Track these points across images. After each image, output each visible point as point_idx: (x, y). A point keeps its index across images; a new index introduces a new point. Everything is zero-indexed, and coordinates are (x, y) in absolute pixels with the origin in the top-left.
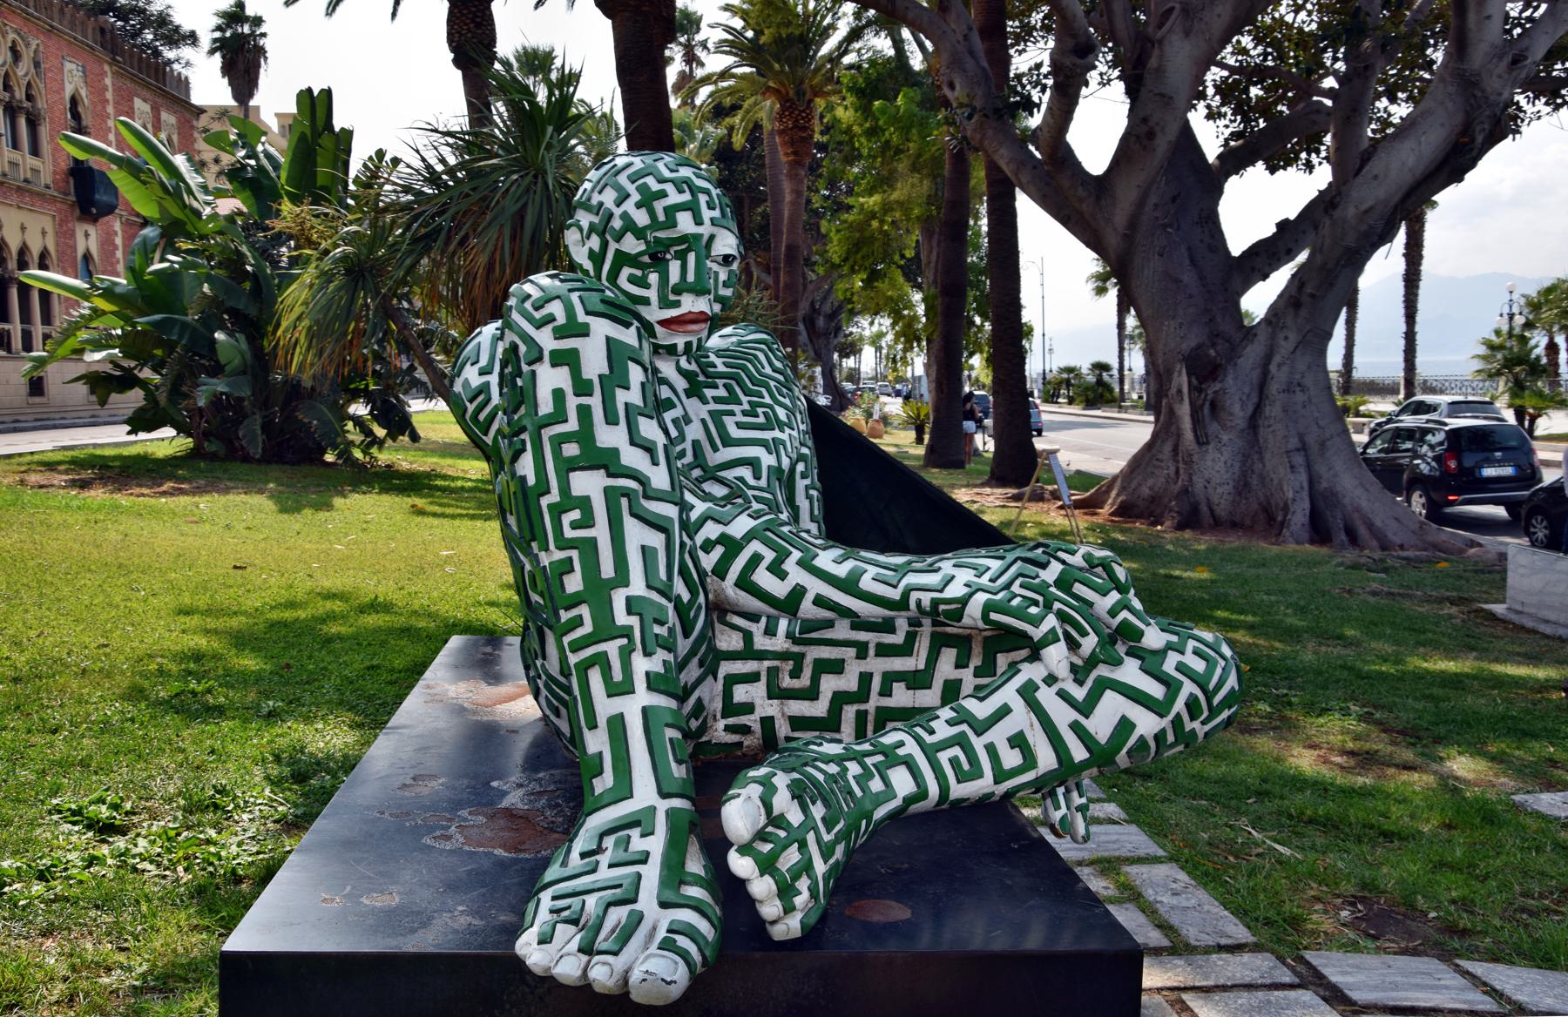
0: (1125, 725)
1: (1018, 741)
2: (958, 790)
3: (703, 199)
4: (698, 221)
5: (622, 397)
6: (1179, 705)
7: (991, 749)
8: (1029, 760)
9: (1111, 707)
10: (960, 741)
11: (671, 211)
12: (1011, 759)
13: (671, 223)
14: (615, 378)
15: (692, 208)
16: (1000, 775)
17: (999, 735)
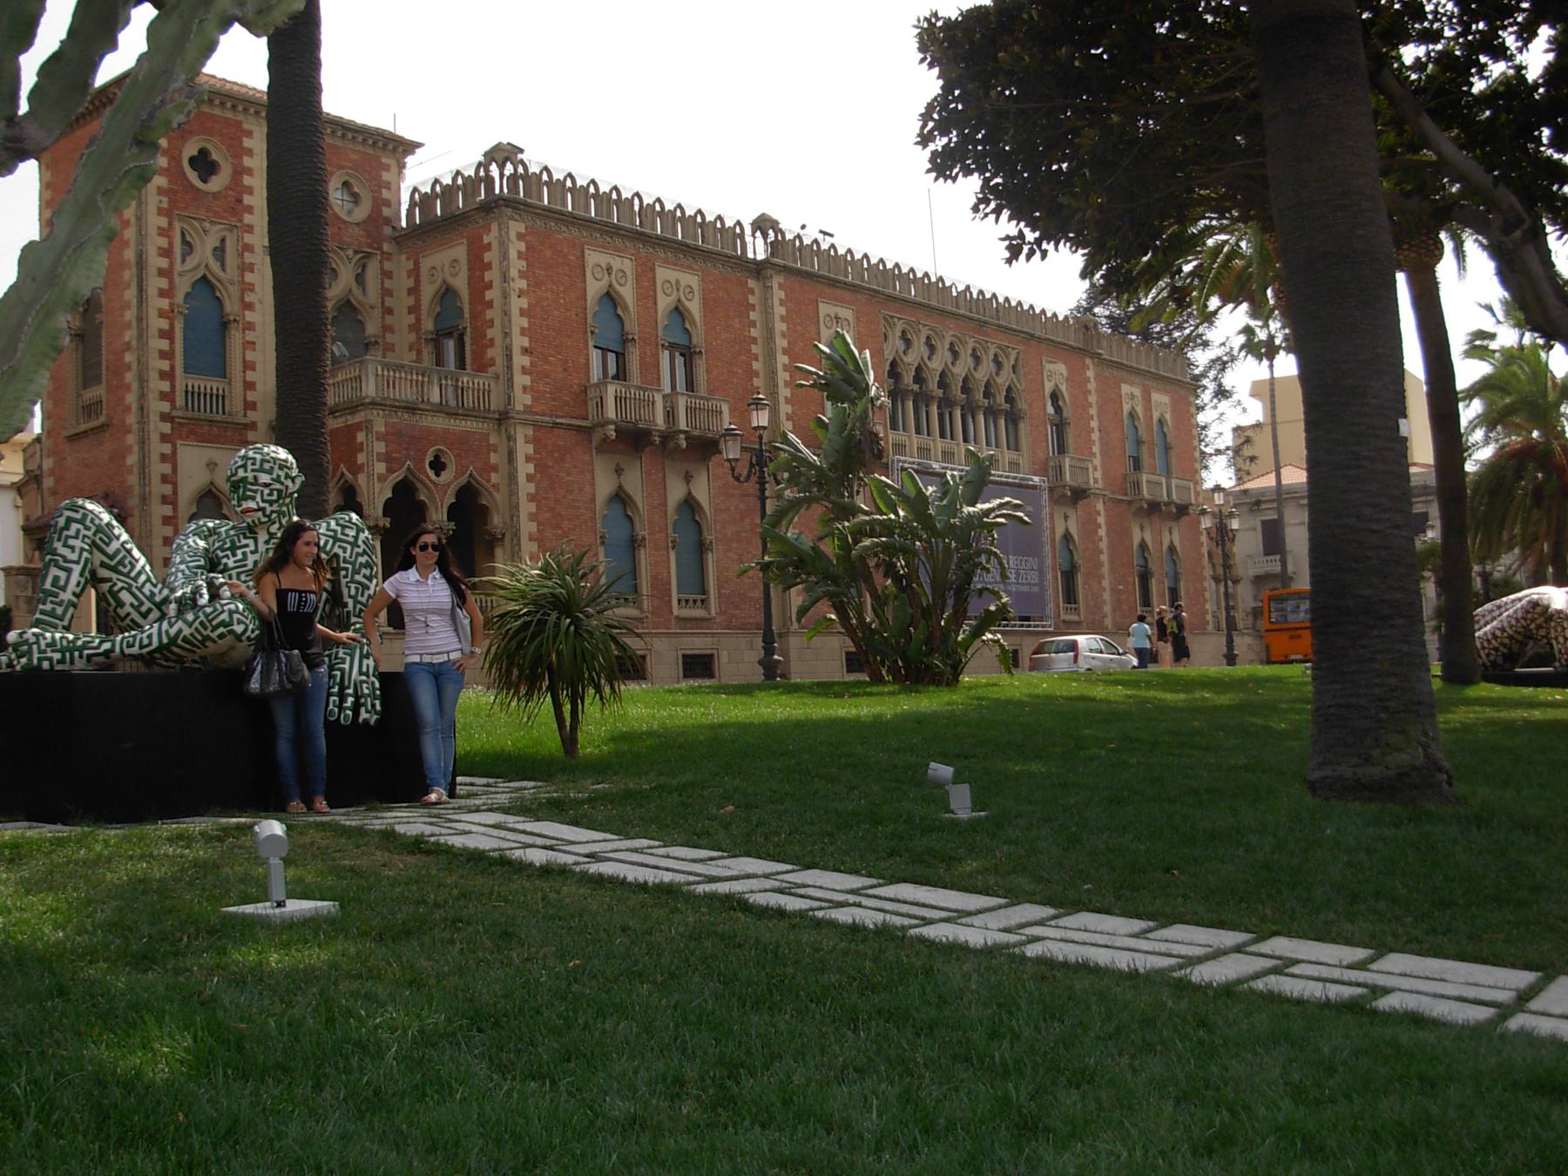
0: (180, 631)
1: (150, 636)
2: (127, 651)
3: (250, 462)
4: (246, 471)
5: (66, 533)
6: (197, 624)
7: (141, 639)
8: (150, 644)
9: (180, 624)
10: (134, 636)
11: (237, 469)
12: (146, 641)
13: (236, 474)
14: (67, 527)
15: (244, 466)
16: (141, 647)
17: (145, 635)
